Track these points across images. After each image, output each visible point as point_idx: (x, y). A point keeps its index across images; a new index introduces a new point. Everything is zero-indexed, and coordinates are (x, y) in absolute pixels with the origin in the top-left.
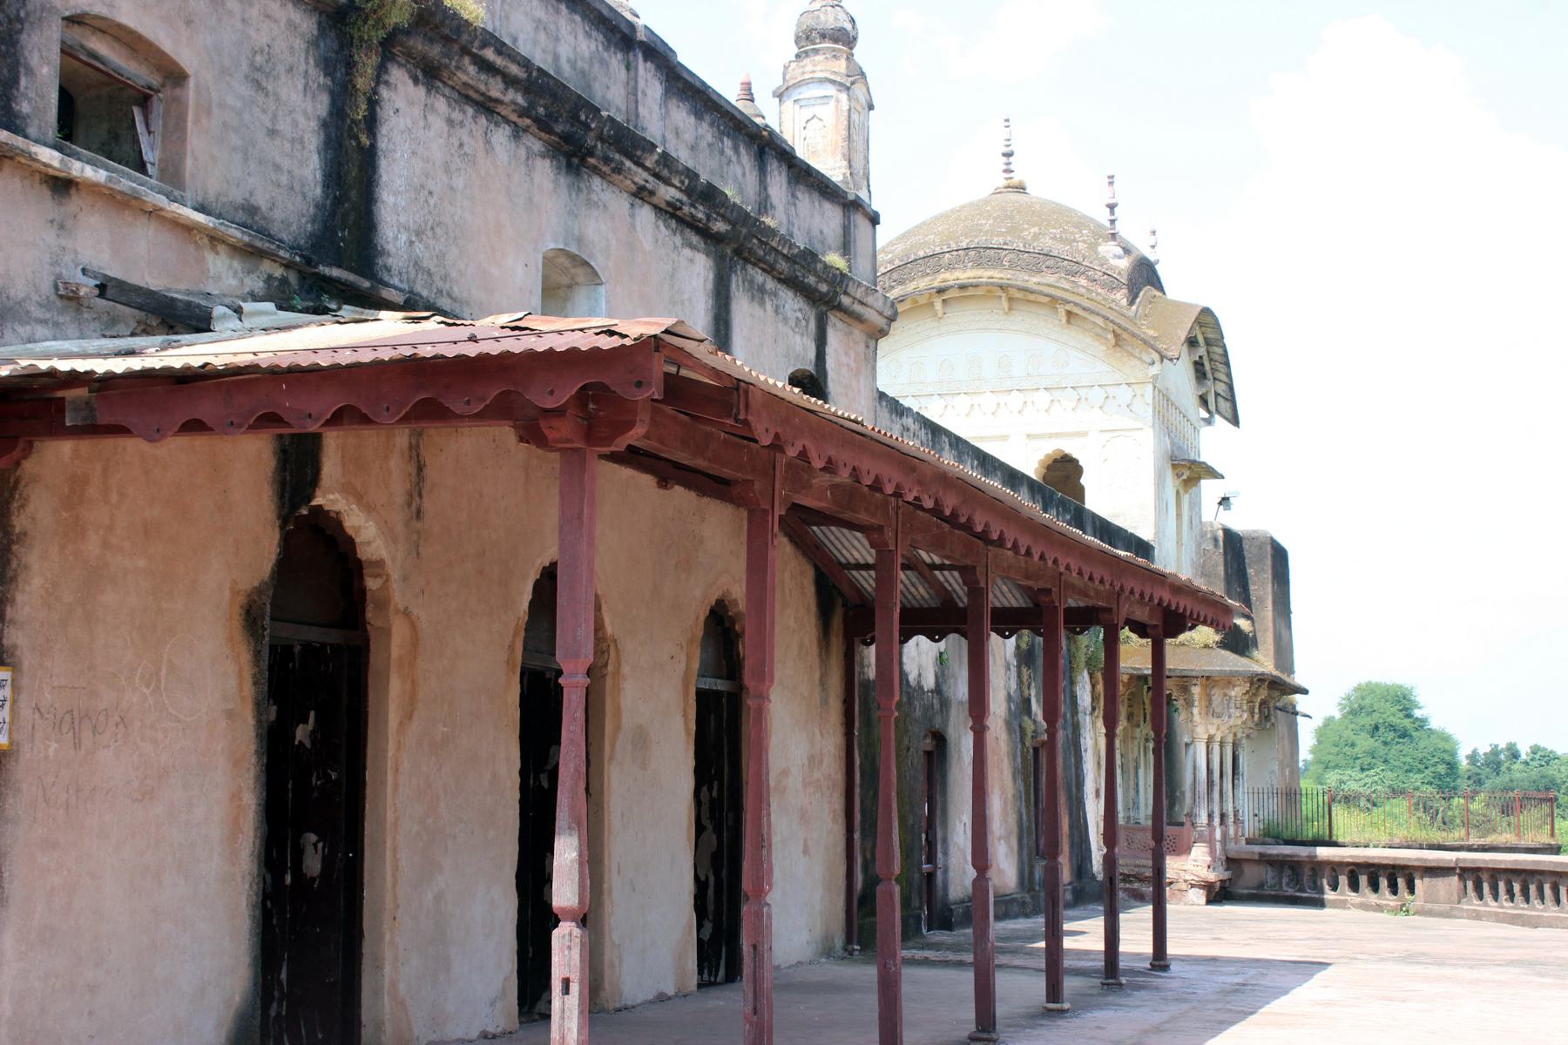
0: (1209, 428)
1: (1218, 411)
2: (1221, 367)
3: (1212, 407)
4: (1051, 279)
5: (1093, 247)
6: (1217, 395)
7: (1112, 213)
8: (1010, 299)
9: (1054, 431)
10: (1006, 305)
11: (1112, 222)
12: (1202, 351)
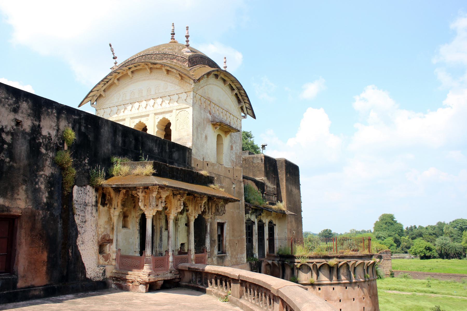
1: (248, 113)
2: (246, 98)
3: (246, 112)
4: (164, 61)
5: (180, 50)
6: (246, 108)
7: (187, 39)
8: (151, 69)
9: (162, 111)
10: (149, 70)
12: (236, 91)
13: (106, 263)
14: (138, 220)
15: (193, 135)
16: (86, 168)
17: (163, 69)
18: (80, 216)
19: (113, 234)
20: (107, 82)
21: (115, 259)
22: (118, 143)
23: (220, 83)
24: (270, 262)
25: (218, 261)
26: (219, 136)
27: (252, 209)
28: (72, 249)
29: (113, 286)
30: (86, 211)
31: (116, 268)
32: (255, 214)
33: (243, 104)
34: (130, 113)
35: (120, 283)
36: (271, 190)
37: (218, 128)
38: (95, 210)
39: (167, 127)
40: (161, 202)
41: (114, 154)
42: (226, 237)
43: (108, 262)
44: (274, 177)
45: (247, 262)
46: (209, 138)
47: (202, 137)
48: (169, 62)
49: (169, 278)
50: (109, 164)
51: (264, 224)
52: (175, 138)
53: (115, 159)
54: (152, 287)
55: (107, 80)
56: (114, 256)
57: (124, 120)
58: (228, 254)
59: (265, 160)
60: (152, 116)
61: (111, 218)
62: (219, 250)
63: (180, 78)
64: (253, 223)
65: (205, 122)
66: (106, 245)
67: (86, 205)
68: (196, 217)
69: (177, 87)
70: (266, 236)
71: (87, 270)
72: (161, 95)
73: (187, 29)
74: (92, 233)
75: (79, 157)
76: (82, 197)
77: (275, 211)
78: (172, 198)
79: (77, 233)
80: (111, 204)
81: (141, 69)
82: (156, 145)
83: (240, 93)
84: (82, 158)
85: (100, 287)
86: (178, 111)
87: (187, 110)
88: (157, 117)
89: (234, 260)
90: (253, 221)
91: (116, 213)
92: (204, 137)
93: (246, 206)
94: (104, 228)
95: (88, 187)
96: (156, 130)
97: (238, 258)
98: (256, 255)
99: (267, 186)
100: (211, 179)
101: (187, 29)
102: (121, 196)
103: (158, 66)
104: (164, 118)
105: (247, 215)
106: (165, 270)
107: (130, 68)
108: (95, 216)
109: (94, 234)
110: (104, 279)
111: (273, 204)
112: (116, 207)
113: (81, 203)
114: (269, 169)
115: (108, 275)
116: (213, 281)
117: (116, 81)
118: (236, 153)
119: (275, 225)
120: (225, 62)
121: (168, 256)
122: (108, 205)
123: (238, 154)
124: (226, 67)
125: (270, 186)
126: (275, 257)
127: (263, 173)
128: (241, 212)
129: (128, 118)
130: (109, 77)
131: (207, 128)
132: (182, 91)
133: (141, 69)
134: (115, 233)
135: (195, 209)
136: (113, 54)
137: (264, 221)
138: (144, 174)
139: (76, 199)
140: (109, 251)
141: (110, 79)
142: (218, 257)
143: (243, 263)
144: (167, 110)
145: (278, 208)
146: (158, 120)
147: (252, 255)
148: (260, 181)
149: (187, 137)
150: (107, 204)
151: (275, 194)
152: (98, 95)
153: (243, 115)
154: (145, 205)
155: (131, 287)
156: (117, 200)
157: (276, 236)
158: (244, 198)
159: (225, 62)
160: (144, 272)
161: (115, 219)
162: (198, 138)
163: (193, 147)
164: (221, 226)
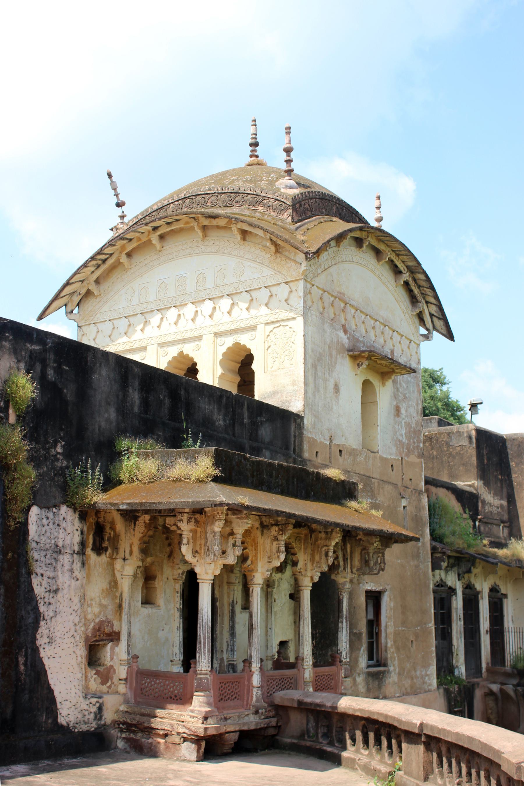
0: (426, 342)
1: (434, 328)
2: (429, 292)
4: (236, 210)
5: (272, 183)
6: (431, 315)
7: (288, 155)
8: (204, 228)
9: (233, 327)
11: (289, 162)
12: (406, 276)
13: (104, 688)
14: (178, 587)
15: (306, 384)
16: (59, 464)
17: (234, 228)
18: (45, 578)
19: (120, 620)
20: (104, 261)
21: (126, 680)
22: (132, 405)
23: (368, 258)
24: (495, 688)
25: (367, 684)
26: (366, 384)
27: (449, 557)
28: (26, 656)
29: (120, 744)
30: (59, 566)
31: (126, 702)
32: (455, 569)
33: (422, 306)
34: (156, 332)
35: (140, 740)
36: (495, 510)
37: (364, 366)
38: (79, 564)
39: (243, 365)
40: (234, 545)
41: (123, 432)
42: (386, 626)
43: (110, 687)
44: (501, 481)
45: (438, 687)
46: (342, 389)
47: (326, 388)
48: (247, 212)
49: (252, 727)
50: (111, 456)
51: (478, 593)
52: (262, 391)
53: (125, 443)
54: (212, 748)
55: (103, 257)
56: (122, 672)
57: (144, 349)
58: (391, 668)
59: (477, 440)
60: (208, 339)
61: (116, 582)
62: (370, 657)
63: (273, 248)
64: (452, 591)
65: (334, 352)
66: (105, 645)
67: (58, 551)
68: (316, 579)
69: (267, 271)
70: (485, 624)
71: (59, 706)
72: (228, 291)
73: (288, 133)
74: (71, 618)
75: (42, 439)
76: (48, 534)
77: (504, 563)
78: (259, 533)
79: (37, 617)
80: (116, 549)
81: (181, 230)
82: (219, 410)
83: (415, 280)
84: (48, 442)
85: (92, 745)
86: (270, 327)
87: (290, 323)
88: (220, 340)
89: (407, 683)
90: (450, 588)
91: (127, 570)
92: (331, 386)
93: (434, 549)
94: (101, 605)
95: (64, 509)
96: (219, 371)
97: (417, 677)
98: (461, 669)
99: (483, 502)
100: (350, 489)
101: (288, 133)
102: (140, 529)
103: (222, 222)
104: (237, 345)
105: (437, 572)
106: (243, 706)
107: (155, 229)
108: (80, 576)
109: (77, 620)
110: (99, 727)
111: (500, 545)
112: (127, 556)
113: (48, 546)
114: (489, 459)
115: (109, 716)
116: (359, 735)
117: (124, 259)
118: (408, 425)
119: (505, 596)
120: (378, 208)
121: (251, 674)
122: (109, 551)
123: (413, 425)
124: (380, 220)
125: (492, 501)
126: (508, 675)
127: (474, 471)
128: (422, 566)
129: (152, 345)
130: (108, 250)
131: (338, 366)
132: (279, 278)
133: (181, 230)
134: (125, 617)
135: (312, 560)
136: (117, 195)
137: (478, 587)
138: (193, 478)
139: (36, 538)
140: (112, 659)
141: (111, 255)
142: (369, 674)
143: (429, 691)
144: (243, 325)
145: (513, 555)
146: (224, 349)
147: (451, 669)
148: (468, 489)
149: (291, 387)
150: (106, 549)
151: (503, 522)
152: (83, 291)
153: (426, 332)
154: (195, 552)
155: (162, 747)
156: (131, 539)
157: (508, 623)
158: (428, 531)
159: (378, 208)
160: (192, 711)
161: (125, 585)
162: (317, 389)
163: (307, 411)
164: (374, 598)
